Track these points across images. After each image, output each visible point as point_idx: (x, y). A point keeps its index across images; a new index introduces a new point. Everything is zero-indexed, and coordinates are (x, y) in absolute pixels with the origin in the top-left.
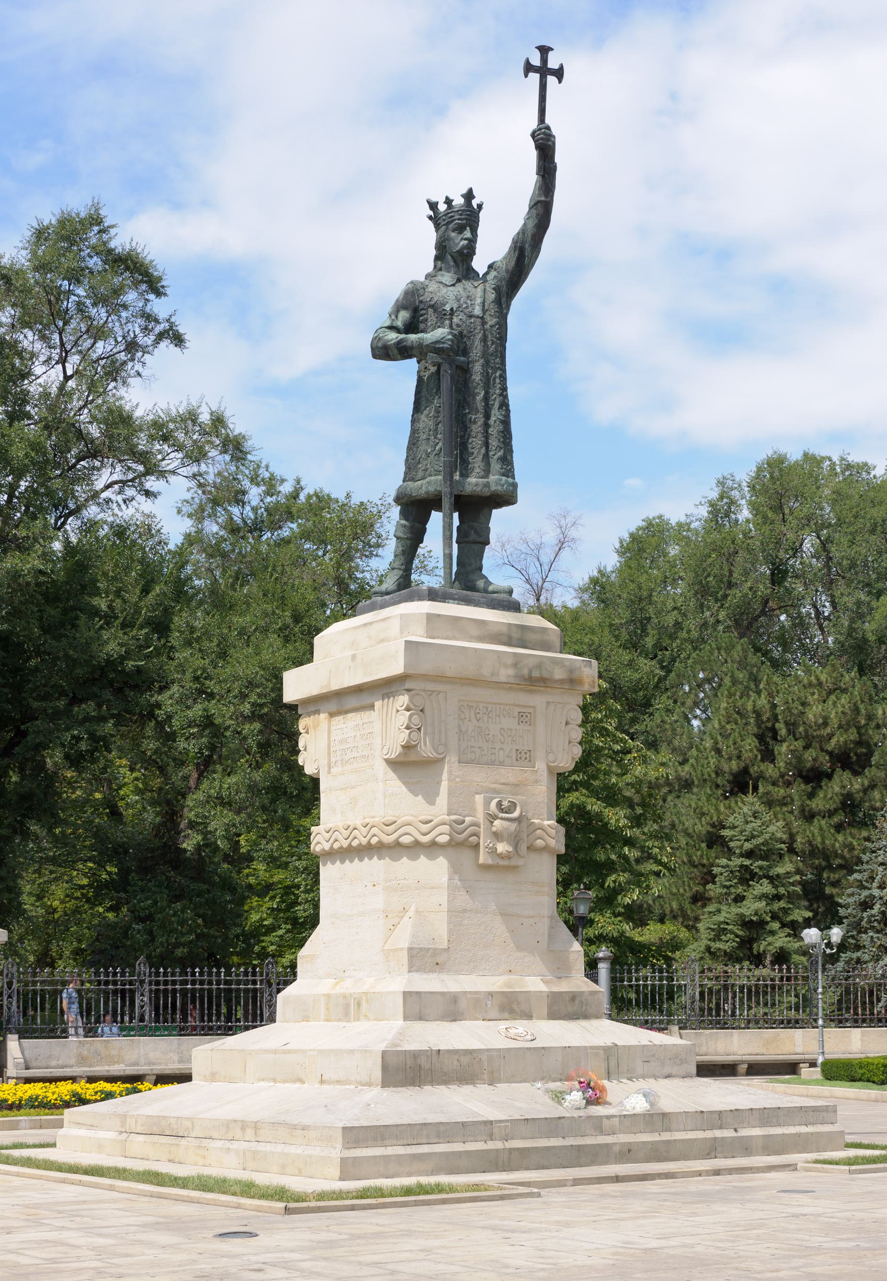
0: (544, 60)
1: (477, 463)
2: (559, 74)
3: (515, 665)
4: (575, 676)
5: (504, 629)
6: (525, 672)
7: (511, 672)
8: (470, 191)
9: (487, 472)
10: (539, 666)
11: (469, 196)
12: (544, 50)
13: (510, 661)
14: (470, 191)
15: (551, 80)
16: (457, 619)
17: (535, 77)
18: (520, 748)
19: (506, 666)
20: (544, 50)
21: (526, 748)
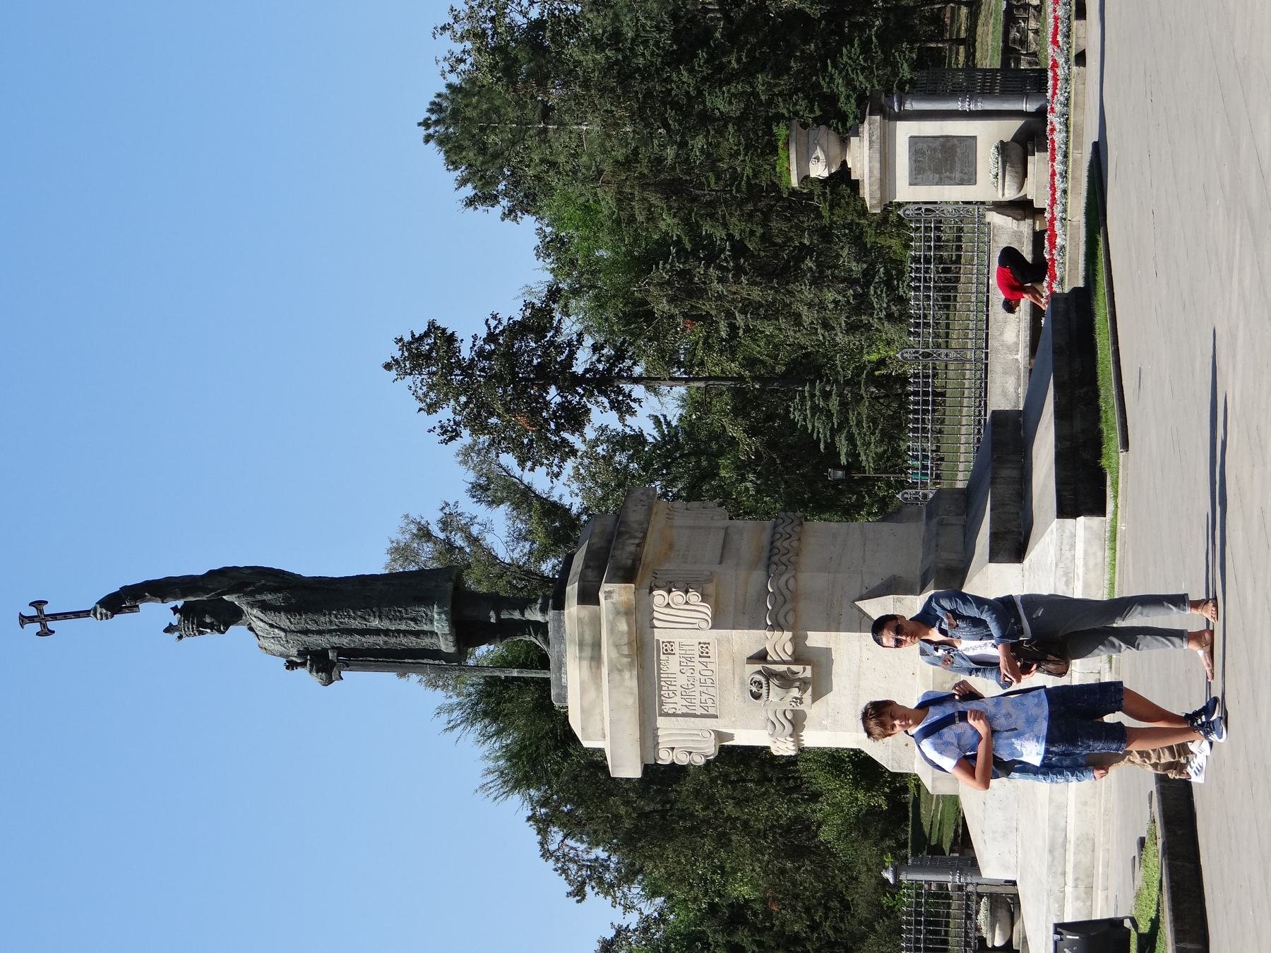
0: (31, 619)
1: (426, 642)
2: (38, 604)
3: (619, 670)
4: (622, 609)
5: (585, 664)
6: (625, 660)
7: (627, 675)
8: (167, 631)
9: (433, 633)
10: (617, 646)
11: (170, 629)
12: (24, 620)
13: (616, 676)
14: (167, 631)
15: (47, 610)
16: (583, 711)
17: (51, 625)
18: (697, 653)
19: (623, 680)
20: (24, 620)
21: (697, 647)
